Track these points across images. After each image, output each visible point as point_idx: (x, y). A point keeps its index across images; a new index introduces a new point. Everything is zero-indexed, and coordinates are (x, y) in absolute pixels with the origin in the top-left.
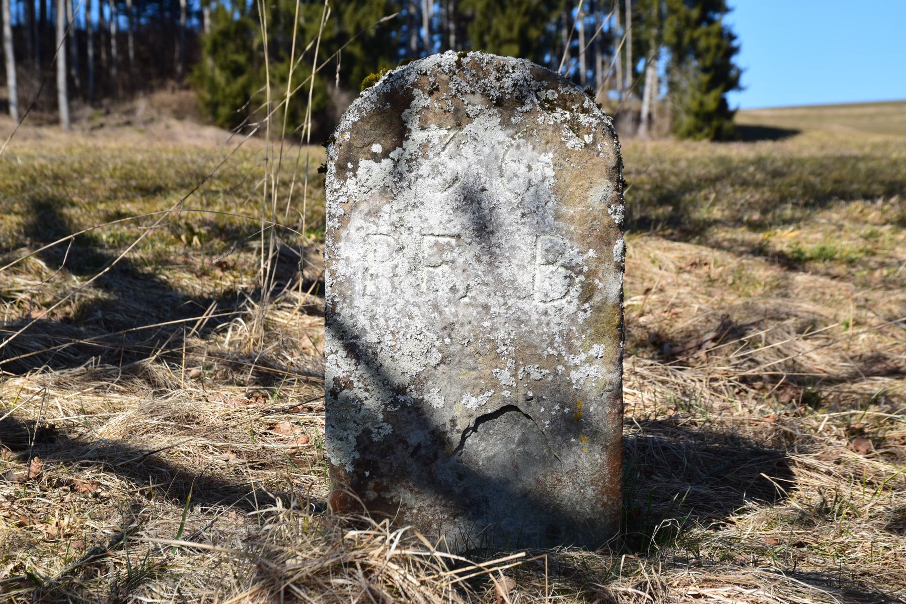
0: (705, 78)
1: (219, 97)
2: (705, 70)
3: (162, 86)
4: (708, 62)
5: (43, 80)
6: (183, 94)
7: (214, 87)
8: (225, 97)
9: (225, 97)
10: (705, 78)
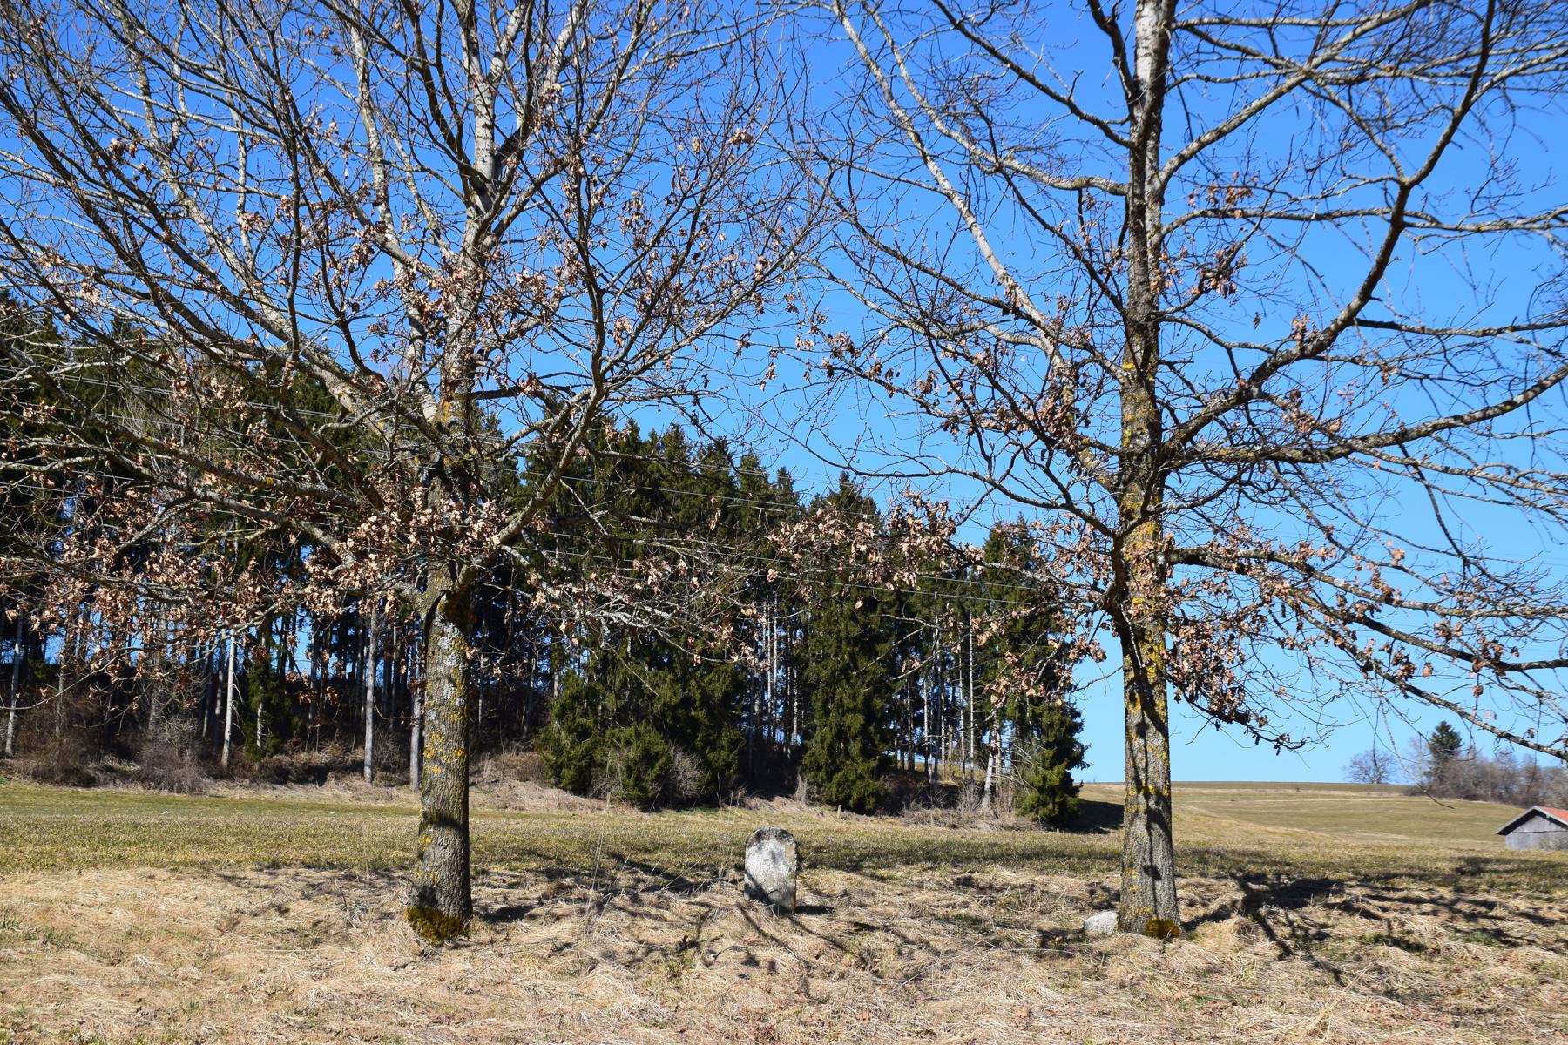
0: (1050, 753)
1: (564, 759)
2: (1049, 746)
3: (508, 747)
4: (1052, 739)
5: (397, 742)
6: (529, 754)
7: (559, 750)
8: (570, 760)
9: (570, 760)
10: (1050, 753)
